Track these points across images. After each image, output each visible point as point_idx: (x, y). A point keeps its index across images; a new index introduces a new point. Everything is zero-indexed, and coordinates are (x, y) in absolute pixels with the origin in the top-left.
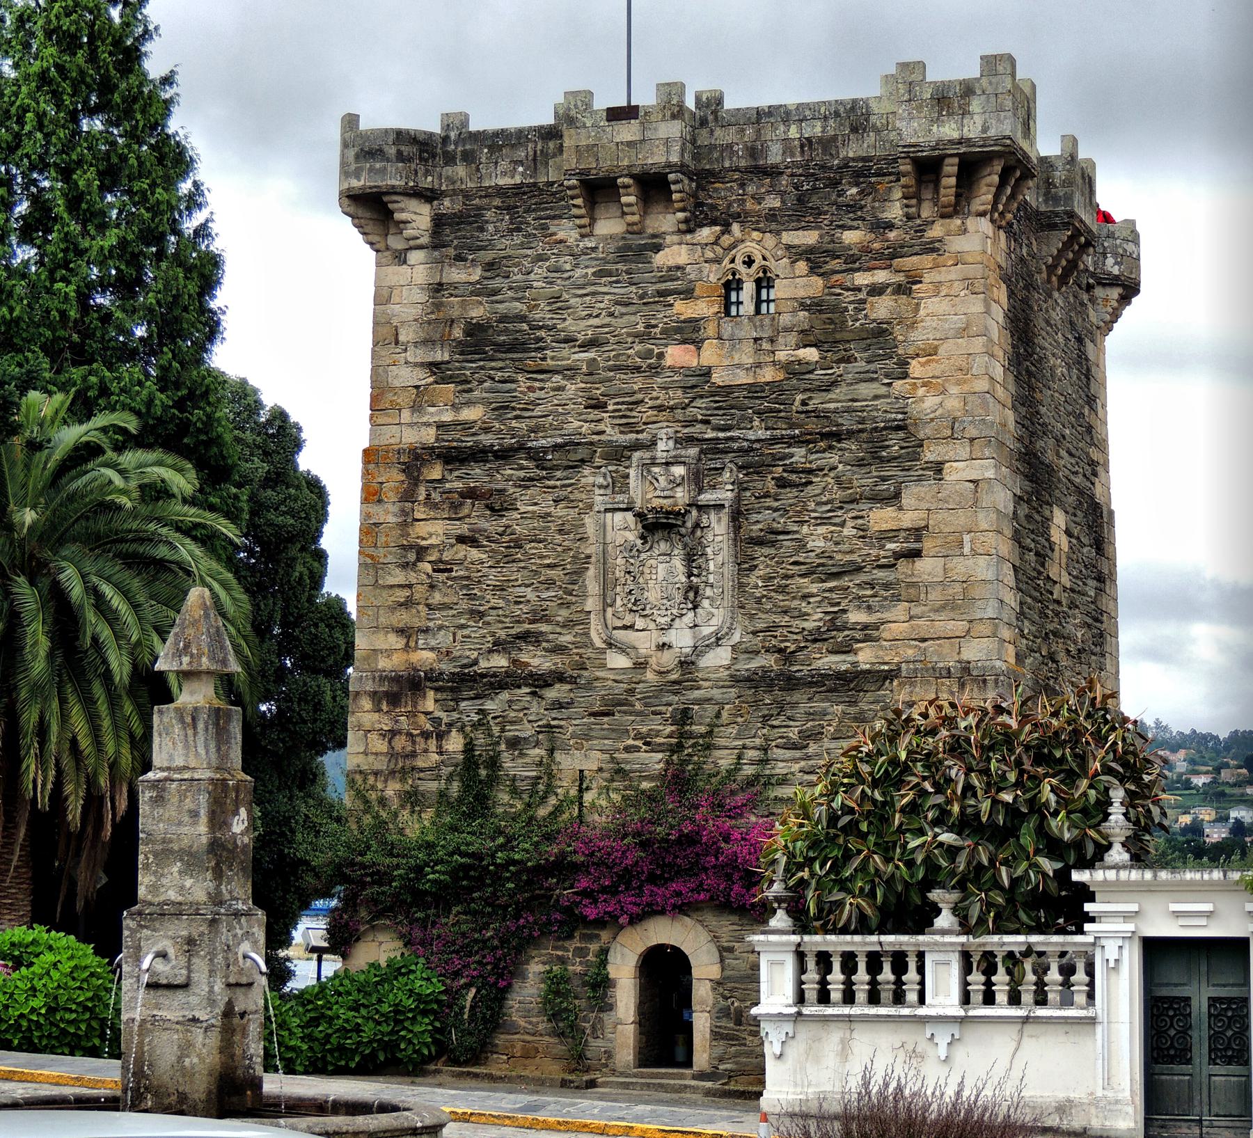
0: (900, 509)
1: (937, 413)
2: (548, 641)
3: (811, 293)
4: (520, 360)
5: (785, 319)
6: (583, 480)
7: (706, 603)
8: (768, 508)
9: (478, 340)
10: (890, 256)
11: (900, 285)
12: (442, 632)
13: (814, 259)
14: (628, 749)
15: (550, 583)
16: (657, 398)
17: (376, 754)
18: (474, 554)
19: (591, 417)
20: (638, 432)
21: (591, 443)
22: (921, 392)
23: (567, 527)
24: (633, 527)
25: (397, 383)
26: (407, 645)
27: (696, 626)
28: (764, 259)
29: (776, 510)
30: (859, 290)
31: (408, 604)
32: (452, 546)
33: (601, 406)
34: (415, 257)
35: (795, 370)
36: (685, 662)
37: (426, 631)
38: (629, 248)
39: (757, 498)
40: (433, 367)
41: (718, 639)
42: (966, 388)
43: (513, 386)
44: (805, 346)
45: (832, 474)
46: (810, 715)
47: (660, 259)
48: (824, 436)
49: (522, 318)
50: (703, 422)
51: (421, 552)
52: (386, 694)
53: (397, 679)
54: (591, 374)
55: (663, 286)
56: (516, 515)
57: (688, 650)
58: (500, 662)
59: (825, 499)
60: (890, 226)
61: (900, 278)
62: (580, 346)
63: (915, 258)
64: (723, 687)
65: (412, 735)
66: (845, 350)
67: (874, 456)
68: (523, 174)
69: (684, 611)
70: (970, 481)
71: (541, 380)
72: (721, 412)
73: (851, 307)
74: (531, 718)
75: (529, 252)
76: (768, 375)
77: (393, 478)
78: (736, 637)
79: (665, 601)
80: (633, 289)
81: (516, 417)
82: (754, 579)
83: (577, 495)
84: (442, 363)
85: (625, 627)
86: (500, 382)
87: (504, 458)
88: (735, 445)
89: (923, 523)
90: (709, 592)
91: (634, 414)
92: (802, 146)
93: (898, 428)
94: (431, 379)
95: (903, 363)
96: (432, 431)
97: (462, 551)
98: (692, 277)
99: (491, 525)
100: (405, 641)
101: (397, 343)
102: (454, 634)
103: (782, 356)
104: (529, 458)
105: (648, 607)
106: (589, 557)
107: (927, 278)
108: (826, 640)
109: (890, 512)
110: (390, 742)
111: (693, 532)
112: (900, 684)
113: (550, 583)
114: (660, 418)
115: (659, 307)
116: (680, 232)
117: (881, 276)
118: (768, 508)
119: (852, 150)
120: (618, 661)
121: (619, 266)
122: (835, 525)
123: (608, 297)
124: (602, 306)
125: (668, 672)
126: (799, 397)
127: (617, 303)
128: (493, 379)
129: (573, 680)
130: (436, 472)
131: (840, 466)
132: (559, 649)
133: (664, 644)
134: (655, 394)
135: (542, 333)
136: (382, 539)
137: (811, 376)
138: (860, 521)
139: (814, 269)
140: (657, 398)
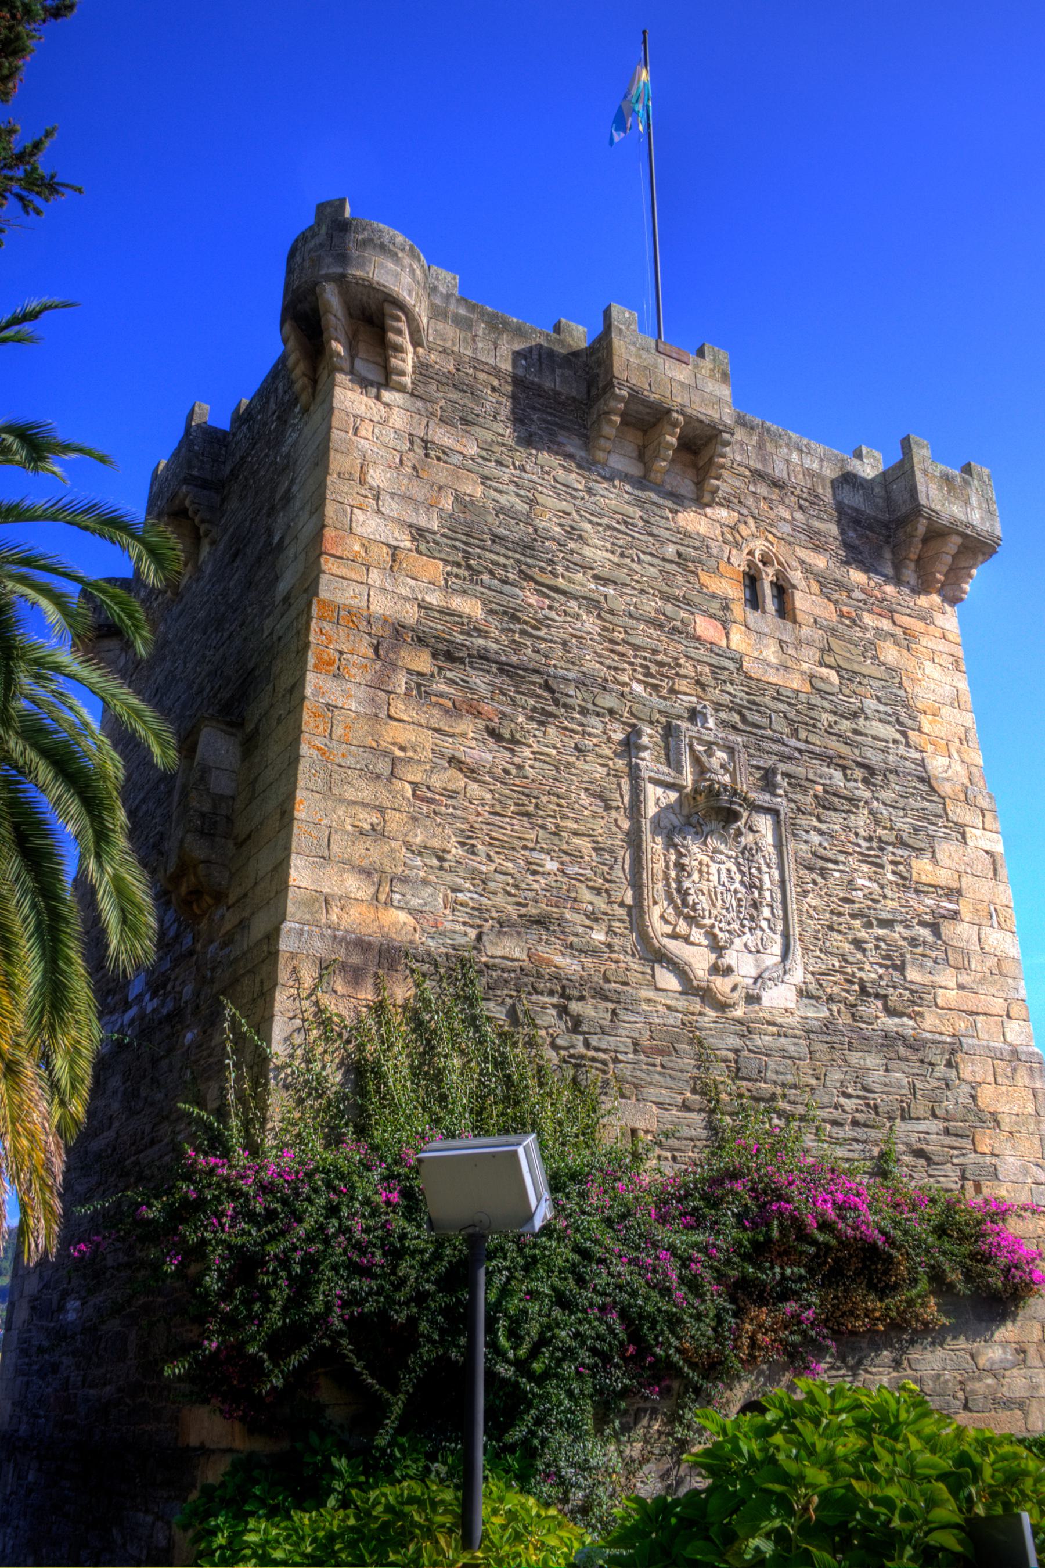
2: (576, 935)
5: (805, 631)
12: (430, 890)
15: (575, 856)
20: (665, 699)
27: (758, 952)
28: (780, 563)
29: (821, 833)
31: (377, 833)
37: (405, 880)
40: (419, 533)
43: (517, 591)
48: (860, 765)
52: (344, 967)
53: (362, 945)
55: (682, 549)
56: (527, 752)
64: (795, 1037)
70: (987, 852)
71: (554, 599)
74: (560, 1042)
76: (795, 682)
79: (724, 912)
81: (523, 633)
85: (674, 936)
87: (508, 673)
88: (775, 747)
89: (954, 885)
94: (408, 544)
97: (459, 781)
99: (503, 758)
100: (372, 890)
101: (362, 482)
102: (445, 896)
103: (805, 666)
104: (547, 687)
117: (886, 624)
118: (815, 829)
130: (423, 662)
132: (592, 952)
136: (339, 731)
137: (833, 698)
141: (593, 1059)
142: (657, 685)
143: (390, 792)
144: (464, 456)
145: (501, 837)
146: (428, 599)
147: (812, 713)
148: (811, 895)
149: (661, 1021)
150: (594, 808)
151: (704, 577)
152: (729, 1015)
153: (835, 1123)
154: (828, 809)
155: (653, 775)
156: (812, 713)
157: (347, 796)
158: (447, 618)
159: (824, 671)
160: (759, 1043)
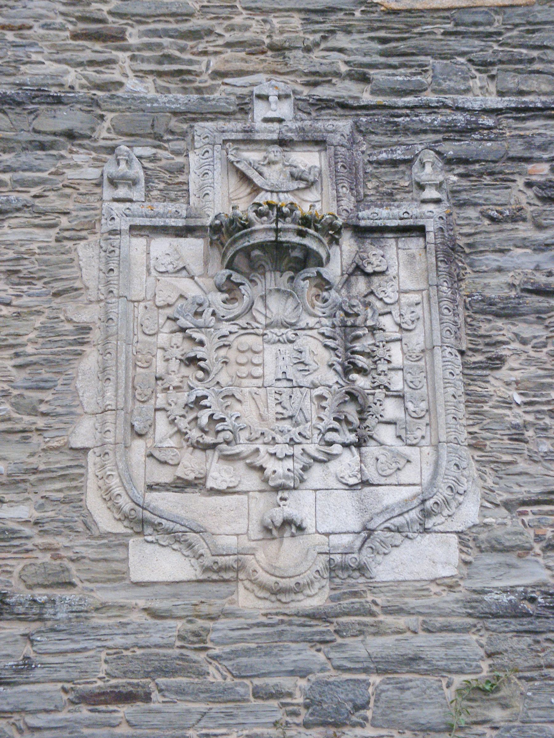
6: (70, 174)
7: (386, 434)
8: (523, 243)
16: (246, 28)
19: (87, 55)
23: (26, 267)
24: (196, 268)
27: (365, 483)
33: (116, 38)
36: (345, 567)
39: (493, 220)
50: (350, 76)
57: (346, 539)
69: (336, 449)
79: (286, 425)
82: (496, 385)
83: (54, 201)
90: (391, 409)
91: (187, 56)
105: (243, 436)
106: (86, 329)
114: (250, 67)
118: (523, 243)
120: (159, 563)
125: (298, 589)
129: (36, 612)
133: (287, 522)
134: (238, 20)
140: (246, 28)
142: (180, 72)
147: (536, 38)
148: (512, 363)
149: (130, 640)
150: (25, 300)
152: (294, 607)
155: (139, 221)
156: (536, 38)
160: (362, 653)
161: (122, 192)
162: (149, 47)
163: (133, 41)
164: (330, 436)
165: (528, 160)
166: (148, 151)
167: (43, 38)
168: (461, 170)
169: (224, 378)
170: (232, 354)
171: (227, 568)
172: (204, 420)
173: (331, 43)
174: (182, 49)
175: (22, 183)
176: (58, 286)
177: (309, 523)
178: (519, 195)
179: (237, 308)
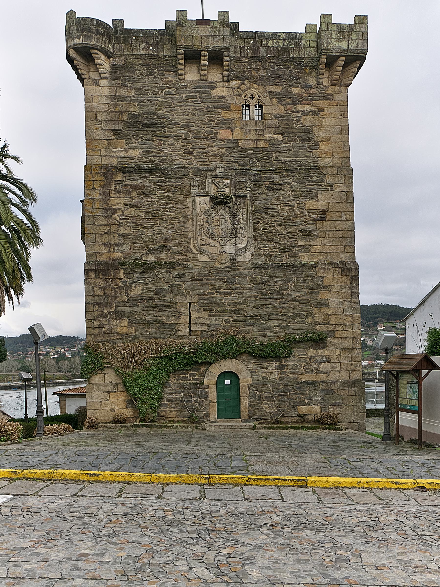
0: (317, 201)
1: (331, 164)
3: (279, 112)
4: (154, 131)
7: (240, 236)
8: (264, 199)
9: (133, 122)
10: (310, 100)
11: (315, 112)
13: (280, 98)
14: (209, 294)
16: (216, 151)
17: (98, 296)
18: (138, 213)
20: (207, 165)
21: (189, 168)
22: (324, 155)
25: (97, 138)
26: (109, 250)
27: (236, 245)
30: (299, 112)
32: (128, 209)
33: (191, 153)
34: (103, 82)
35: (272, 143)
38: (201, 87)
41: (246, 250)
42: (341, 155)
44: (277, 134)
45: (289, 186)
46: (284, 282)
47: (214, 92)
49: (154, 114)
50: (234, 162)
51: (114, 211)
53: (106, 264)
54: (186, 139)
55: (216, 104)
58: (152, 258)
59: (286, 196)
60: (311, 87)
61: (315, 109)
62: (180, 127)
63: (320, 101)
65: (114, 288)
66: (293, 137)
67: (307, 180)
68: (152, 50)
70: (344, 192)
71: (164, 141)
72: (242, 159)
73: (295, 119)
75: (156, 85)
76: (262, 144)
77: (99, 179)
78: (253, 250)
79: (223, 234)
80: (203, 104)
84: (118, 130)
85: (206, 245)
86: (145, 140)
87: (149, 173)
89: (326, 208)
91: (204, 157)
92: (274, 50)
93: (316, 169)
94: (113, 137)
95: (317, 144)
96: (116, 160)
98: (229, 101)
100: (109, 249)
101: (97, 120)
103: (267, 137)
107: (326, 110)
108: (288, 252)
109: (313, 202)
110: (104, 291)
111: (234, 207)
112: (319, 270)
113: (172, 225)
115: (215, 113)
116: (224, 81)
117: (307, 108)
118: (264, 199)
119: (294, 54)
120: (203, 258)
121: (197, 94)
122: (291, 206)
123: (191, 107)
124: (190, 111)
125: (226, 263)
126: (274, 155)
127: (197, 110)
128: (142, 139)
130: (119, 177)
131: (293, 183)
134: (214, 149)
135: (164, 121)
138: (301, 205)
139: (280, 102)
141: (177, 285)
143: (112, 219)
144: (130, 97)
145: (147, 225)
146: (120, 155)
151: (224, 113)
153: (262, 294)
154: (271, 190)
157: (99, 224)
158: (127, 159)
159: (275, 136)
161: (194, 188)
162: (198, 155)
163: (195, 154)
164: (230, 236)
165: (266, 181)
166: (198, 179)
167: (179, 154)
168: (254, 183)
169: (213, 225)
170: (214, 221)
171: (214, 259)
172: (210, 234)
173: (231, 155)
174: (204, 156)
175: (177, 185)
176: (184, 207)
177: (227, 252)
178: (264, 189)
179: (215, 212)
